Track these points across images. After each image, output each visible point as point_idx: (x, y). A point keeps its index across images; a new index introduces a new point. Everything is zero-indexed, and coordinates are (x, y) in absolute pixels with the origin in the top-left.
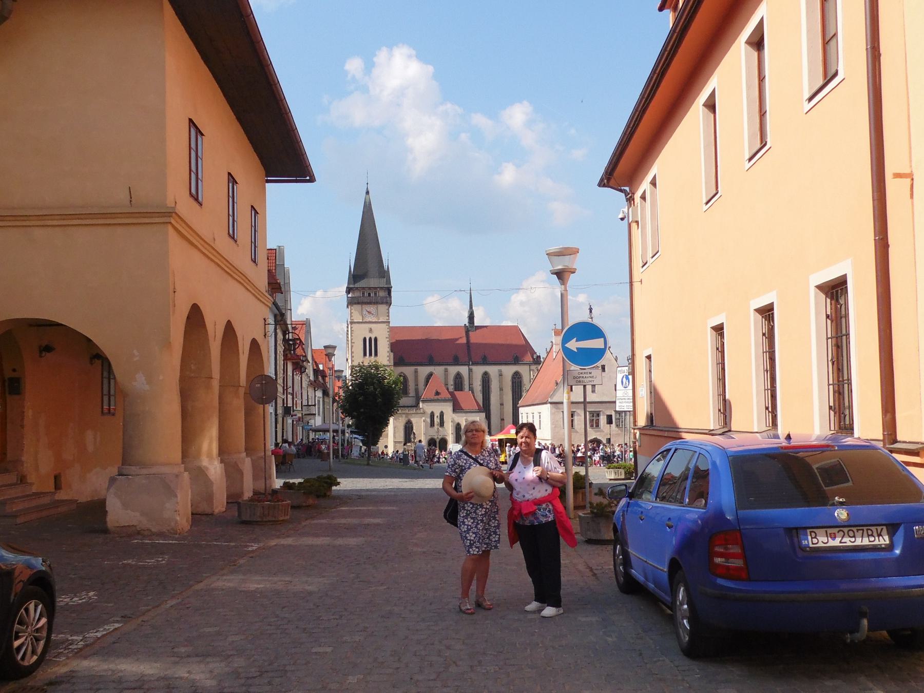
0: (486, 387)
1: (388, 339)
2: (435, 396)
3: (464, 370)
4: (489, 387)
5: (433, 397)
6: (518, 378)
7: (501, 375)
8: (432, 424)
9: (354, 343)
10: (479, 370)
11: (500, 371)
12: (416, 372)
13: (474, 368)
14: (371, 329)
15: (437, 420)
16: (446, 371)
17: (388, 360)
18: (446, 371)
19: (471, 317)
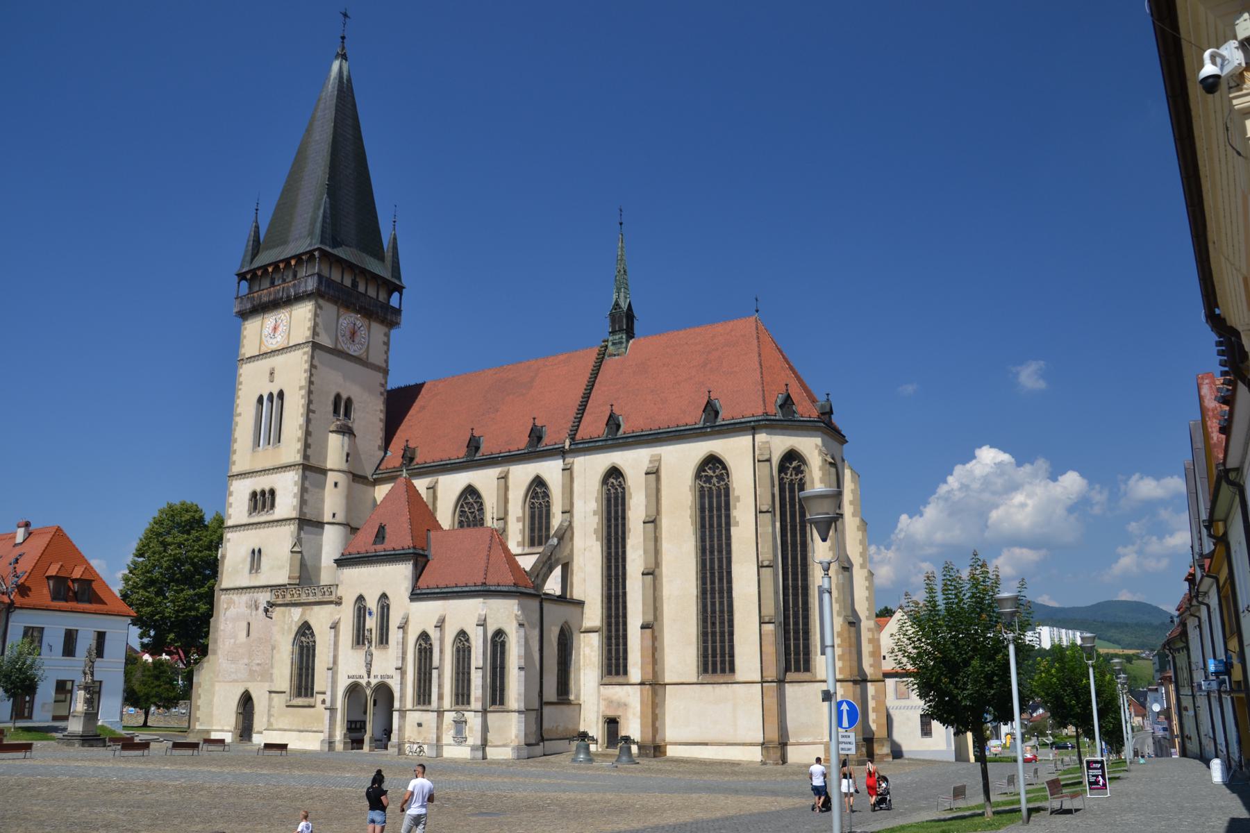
2: (375, 543)
3: (551, 470)
4: (624, 518)
6: (720, 478)
8: (360, 638)
9: (240, 415)
10: (590, 468)
11: (657, 460)
14: (273, 369)
15: (371, 623)
16: (504, 478)
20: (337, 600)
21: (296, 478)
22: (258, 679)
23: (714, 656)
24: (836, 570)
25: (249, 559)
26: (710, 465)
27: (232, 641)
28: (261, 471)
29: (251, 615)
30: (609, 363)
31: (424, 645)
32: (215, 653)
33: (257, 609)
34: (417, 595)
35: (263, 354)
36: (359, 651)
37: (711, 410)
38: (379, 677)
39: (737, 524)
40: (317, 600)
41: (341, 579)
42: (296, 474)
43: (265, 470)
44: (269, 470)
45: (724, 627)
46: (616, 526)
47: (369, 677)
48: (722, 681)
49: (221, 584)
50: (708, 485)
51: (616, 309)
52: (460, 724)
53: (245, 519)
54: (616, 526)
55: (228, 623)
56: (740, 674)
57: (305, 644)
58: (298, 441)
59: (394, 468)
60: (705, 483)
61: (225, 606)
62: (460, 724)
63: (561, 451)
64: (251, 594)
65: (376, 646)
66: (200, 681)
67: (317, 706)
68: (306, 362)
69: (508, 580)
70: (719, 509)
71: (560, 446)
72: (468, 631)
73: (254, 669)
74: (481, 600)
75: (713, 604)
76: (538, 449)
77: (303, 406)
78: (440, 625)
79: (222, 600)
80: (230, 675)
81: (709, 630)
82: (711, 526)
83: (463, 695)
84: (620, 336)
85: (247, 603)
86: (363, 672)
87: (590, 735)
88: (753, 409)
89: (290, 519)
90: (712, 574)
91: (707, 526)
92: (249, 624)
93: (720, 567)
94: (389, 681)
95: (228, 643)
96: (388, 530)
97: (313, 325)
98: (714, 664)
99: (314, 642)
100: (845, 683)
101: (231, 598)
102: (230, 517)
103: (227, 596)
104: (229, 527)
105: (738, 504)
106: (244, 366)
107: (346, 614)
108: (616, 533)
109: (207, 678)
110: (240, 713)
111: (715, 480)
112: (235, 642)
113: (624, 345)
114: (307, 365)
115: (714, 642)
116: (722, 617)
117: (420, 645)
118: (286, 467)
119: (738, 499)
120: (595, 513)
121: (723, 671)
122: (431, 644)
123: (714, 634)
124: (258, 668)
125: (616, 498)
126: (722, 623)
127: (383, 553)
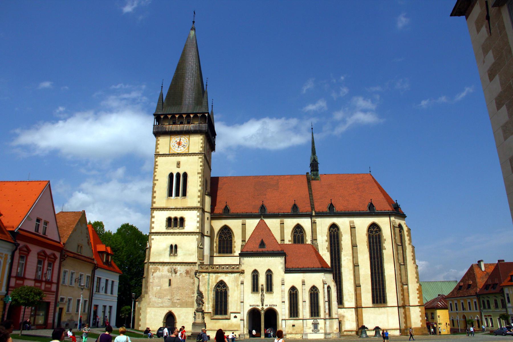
0: (335, 244)
1: (200, 175)
3: (306, 223)
5: (255, 247)
6: (376, 232)
7: (353, 228)
8: (255, 288)
9: (157, 180)
12: (244, 225)
13: (318, 220)
14: (179, 162)
16: (282, 223)
17: (199, 202)
18: (282, 223)
19: (314, 165)
20: (242, 271)
21: (198, 214)
22: (179, 306)
23: (377, 297)
24: (415, 267)
25: (169, 249)
26: (372, 227)
27: (159, 288)
28: (174, 208)
29: (172, 276)
30: (313, 183)
31: (292, 292)
32: (146, 293)
33: (176, 273)
34: (288, 271)
35: (172, 154)
36: (256, 294)
37: (371, 206)
38: (269, 306)
39: (385, 249)
40: (230, 271)
41: (243, 262)
42: (198, 212)
43: (177, 208)
44: (180, 208)
45: (380, 287)
46: (335, 246)
47: (263, 305)
48: (382, 306)
49: (149, 259)
50: (371, 234)
51: (314, 162)
52: (316, 325)
53: (164, 230)
54: (335, 246)
55: (155, 279)
56: (389, 305)
57: (219, 291)
58: (198, 197)
59: (220, 213)
60: (370, 233)
61: (153, 271)
62: (316, 325)
63: (311, 215)
64: (171, 266)
65: (266, 293)
66: (141, 306)
67: (231, 318)
68: (201, 162)
69: (318, 265)
70: (376, 243)
71: (309, 213)
72: (317, 286)
73: (175, 301)
74: (323, 274)
75: (376, 278)
76: (298, 213)
77: (200, 182)
78: (303, 283)
79: (150, 268)
80: (158, 304)
81: (375, 287)
82: (374, 249)
83: (315, 313)
84: (316, 172)
85: (168, 270)
86: (259, 303)
87: (366, 327)
88: (389, 208)
89: (196, 233)
90: (375, 267)
91: (372, 249)
92: (170, 280)
93: (378, 264)
94: (275, 307)
95: (156, 289)
96: (265, 242)
97: (204, 146)
98: (377, 300)
99: (225, 290)
100: (421, 307)
101: (157, 267)
102: (153, 228)
103: (154, 266)
104: (153, 233)
105: (385, 242)
106: (159, 158)
107: (248, 279)
108: (335, 249)
109: (144, 306)
110: (165, 322)
111: (374, 232)
112: (160, 289)
113: (318, 176)
114: (202, 163)
115: (377, 292)
116: (379, 283)
117: (290, 292)
118: (192, 208)
119: (385, 240)
120: (326, 241)
121: (381, 303)
122: (296, 292)
123: (376, 289)
124: (178, 301)
125: (334, 236)
126: (379, 285)
127: (267, 252)
